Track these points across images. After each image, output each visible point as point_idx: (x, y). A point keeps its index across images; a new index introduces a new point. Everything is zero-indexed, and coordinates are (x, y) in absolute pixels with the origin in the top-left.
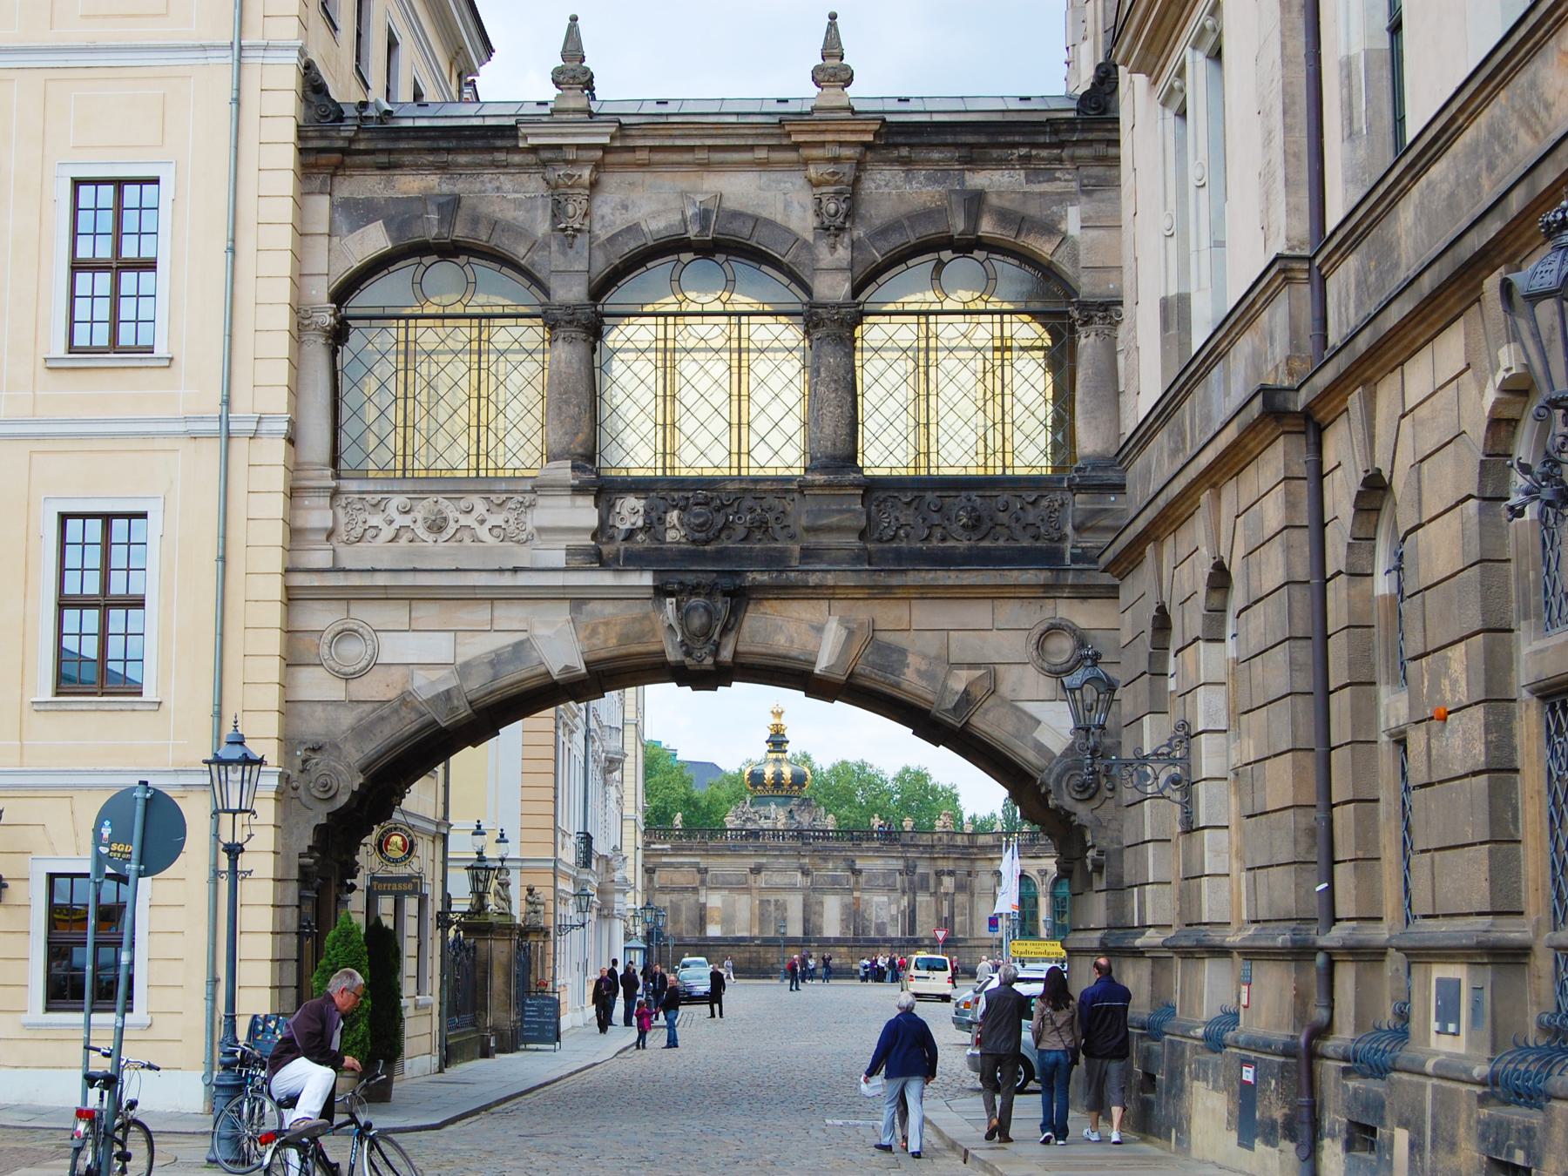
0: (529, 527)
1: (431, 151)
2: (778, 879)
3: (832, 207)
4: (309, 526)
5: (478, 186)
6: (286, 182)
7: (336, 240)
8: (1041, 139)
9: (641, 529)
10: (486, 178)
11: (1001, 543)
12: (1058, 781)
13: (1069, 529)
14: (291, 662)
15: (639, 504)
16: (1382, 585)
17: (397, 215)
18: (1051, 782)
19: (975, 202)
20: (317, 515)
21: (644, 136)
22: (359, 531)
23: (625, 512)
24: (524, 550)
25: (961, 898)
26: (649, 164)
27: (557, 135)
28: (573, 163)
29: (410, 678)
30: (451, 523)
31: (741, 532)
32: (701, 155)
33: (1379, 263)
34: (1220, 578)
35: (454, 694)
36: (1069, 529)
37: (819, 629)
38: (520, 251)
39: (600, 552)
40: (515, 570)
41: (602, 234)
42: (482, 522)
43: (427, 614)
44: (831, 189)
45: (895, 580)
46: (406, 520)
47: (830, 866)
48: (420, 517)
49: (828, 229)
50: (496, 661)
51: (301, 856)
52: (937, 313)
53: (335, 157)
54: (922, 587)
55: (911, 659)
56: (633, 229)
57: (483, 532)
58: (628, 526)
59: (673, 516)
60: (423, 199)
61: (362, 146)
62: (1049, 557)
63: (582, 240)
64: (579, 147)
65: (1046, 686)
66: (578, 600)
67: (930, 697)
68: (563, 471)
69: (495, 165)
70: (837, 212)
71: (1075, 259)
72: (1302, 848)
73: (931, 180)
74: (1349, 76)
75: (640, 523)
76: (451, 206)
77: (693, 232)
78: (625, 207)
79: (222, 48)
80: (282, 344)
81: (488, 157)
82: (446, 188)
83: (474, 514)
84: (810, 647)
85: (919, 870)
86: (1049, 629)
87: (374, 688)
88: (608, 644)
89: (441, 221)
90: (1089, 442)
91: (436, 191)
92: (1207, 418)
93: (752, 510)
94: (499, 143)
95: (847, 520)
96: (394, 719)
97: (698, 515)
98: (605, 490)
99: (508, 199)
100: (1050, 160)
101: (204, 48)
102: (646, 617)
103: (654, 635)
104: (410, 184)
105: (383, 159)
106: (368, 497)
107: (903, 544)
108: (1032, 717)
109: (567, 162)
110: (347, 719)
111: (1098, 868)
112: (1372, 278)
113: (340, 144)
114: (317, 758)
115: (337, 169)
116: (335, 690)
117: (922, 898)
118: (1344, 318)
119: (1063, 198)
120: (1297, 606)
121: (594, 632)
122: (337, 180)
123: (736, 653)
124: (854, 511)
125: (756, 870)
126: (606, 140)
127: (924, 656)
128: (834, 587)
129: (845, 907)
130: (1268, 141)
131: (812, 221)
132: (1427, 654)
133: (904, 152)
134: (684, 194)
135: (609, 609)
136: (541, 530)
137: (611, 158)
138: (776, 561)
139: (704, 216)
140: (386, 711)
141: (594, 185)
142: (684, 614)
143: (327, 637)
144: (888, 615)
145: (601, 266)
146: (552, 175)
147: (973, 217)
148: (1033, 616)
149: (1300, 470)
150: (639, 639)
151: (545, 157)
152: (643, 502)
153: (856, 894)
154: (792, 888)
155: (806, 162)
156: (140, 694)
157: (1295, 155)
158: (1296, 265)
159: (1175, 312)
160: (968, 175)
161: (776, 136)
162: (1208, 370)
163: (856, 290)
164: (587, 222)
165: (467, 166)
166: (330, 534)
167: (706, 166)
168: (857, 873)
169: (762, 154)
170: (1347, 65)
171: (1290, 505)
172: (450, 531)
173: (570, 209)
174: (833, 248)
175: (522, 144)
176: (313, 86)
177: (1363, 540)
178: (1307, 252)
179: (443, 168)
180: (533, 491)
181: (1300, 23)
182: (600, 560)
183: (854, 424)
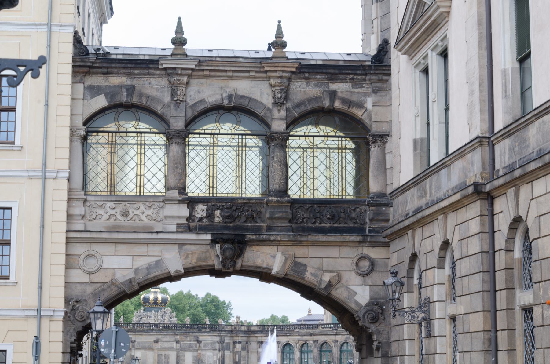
0: (161, 216)
1: (125, 68)
2: (166, 345)
3: (279, 95)
4: (75, 213)
5: (142, 82)
6: (68, 78)
7: (86, 101)
8: (358, 72)
9: (205, 217)
10: (145, 79)
11: (342, 225)
12: (364, 316)
13: (367, 220)
14: (68, 267)
15: (205, 208)
16: (518, 254)
17: (110, 93)
18: (361, 316)
19: (333, 95)
20: (78, 209)
21: (208, 66)
22: (94, 216)
23: (199, 211)
24: (160, 224)
25: (244, 353)
26: (209, 76)
27: (174, 64)
28: (180, 75)
29: (114, 274)
30: (131, 213)
31: (243, 219)
32: (230, 74)
33: (519, 144)
34: (446, 245)
35: (133, 280)
36: (367, 220)
37: (274, 257)
38: (159, 109)
39: (190, 225)
40: (157, 232)
41: (191, 103)
42: (143, 213)
43: (121, 248)
44: (279, 88)
45: (304, 239)
46: (113, 212)
47: (188, 339)
48: (118, 210)
49: (277, 104)
50: (149, 268)
51: (71, 343)
52: (317, 136)
53: (86, 69)
54: (313, 241)
55: (308, 269)
56: (202, 101)
57: (143, 217)
58: (200, 216)
59: (218, 213)
60: (121, 86)
61: (97, 65)
62: (360, 231)
63: (183, 105)
64: (183, 69)
65: (358, 279)
66: (181, 245)
67: (316, 283)
68: (175, 194)
69: (149, 74)
70: (281, 97)
71: (370, 118)
72: (486, 346)
73: (316, 86)
74: (505, 76)
75: (205, 215)
76: (131, 90)
77: (226, 103)
78: (199, 92)
79: (44, 25)
80: (66, 142)
81: (147, 71)
82: (129, 83)
83: (140, 210)
84: (270, 264)
85: (226, 341)
86: (360, 258)
87: (101, 278)
88: (192, 261)
89: (128, 96)
90: (374, 187)
91: (125, 83)
92: (439, 188)
93: (248, 211)
94: (151, 66)
95: (284, 215)
96: (109, 290)
97: (227, 212)
98: (192, 202)
99: (155, 88)
100: (361, 80)
101: (36, 25)
102: (207, 251)
103: (211, 258)
104: (115, 80)
105: (105, 70)
106: (98, 203)
107: (305, 225)
108: (354, 291)
109: (178, 74)
110: (89, 290)
111: (378, 349)
112: (517, 149)
113: (89, 64)
114: (78, 305)
115: (87, 74)
116: (85, 278)
117: (228, 353)
118: (503, 160)
119: (366, 94)
120: (485, 260)
121: (187, 257)
122: (86, 78)
123: (242, 266)
124: (287, 212)
125: (157, 341)
126: (193, 67)
127: (314, 268)
128: (280, 241)
129: (195, 357)
130: (471, 93)
131: (271, 100)
132: (542, 282)
133: (307, 75)
134: (221, 88)
135: (193, 248)
136: (166, 217)
137: (195, 73)
138: (257, 230)
139: (230, 97)
140: (105, 286)
141: (188, 83)
142: (223, 251)
143: (82, 257)
144: (300, 252)
145: (190, 114)
146: (172, 80)
147: (332, 101)
148: (352, 253)
149: (486, 213)
150: (205, 260)
151: (169, 72)
152: (206, 207)
153: (199, 351)
154: (172, 349)
155: (269, 78)
156: (9, 279)
157: (483, 101)
158: (484, 140)
159: (422, 146)
160: (330, 84)
161: (256, 67)
162: (440, 170)
163: (288, 127)
164: (185, 98)
165: (138, 74)
166: (83, 217)
167: (231, 77)
168: (199, 342)
169: (253, 74)
170: (504, 72)
171: (482, 224)
172: (130, 216)
173: (179, 92)
174: (279, 111)
175: (160, 67)
176: (77, 41)
177: (511, 239)
178: (487, 135)
179: (128, 75)
180: (163, 201)
181: (485, 53)
182: (190, 230)
183: (286, 178)
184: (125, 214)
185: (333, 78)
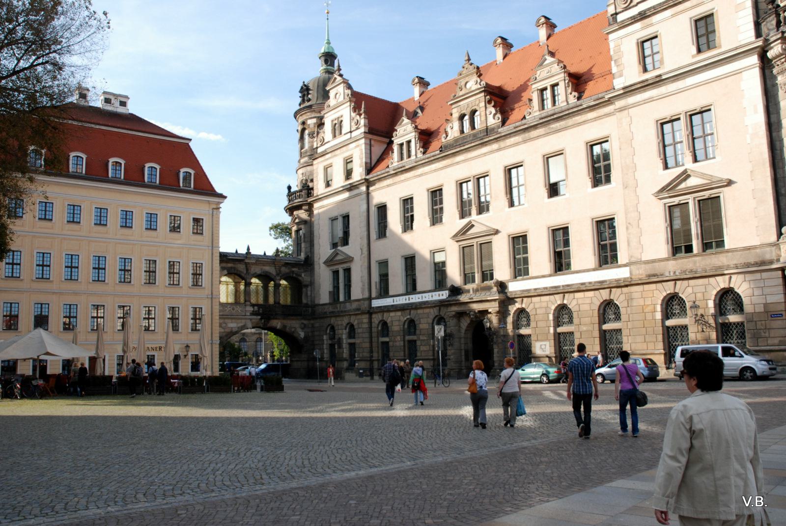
19: (293, 272)
37: (278, 323)
43: (233, 320)
87: (228, 330)
104: (230, 265)
110: (224, 334)
142: (264, 321)
144: (285, 322)
170: (376, 282)
179: (233, 264)
184: (233, 309)
185: (294, 267)
